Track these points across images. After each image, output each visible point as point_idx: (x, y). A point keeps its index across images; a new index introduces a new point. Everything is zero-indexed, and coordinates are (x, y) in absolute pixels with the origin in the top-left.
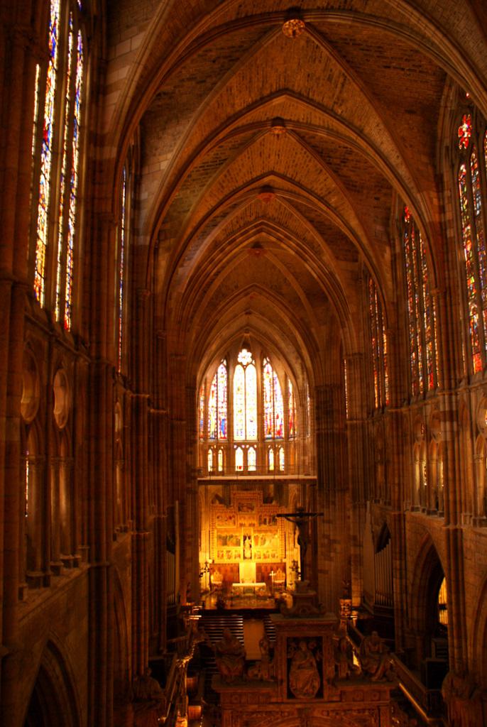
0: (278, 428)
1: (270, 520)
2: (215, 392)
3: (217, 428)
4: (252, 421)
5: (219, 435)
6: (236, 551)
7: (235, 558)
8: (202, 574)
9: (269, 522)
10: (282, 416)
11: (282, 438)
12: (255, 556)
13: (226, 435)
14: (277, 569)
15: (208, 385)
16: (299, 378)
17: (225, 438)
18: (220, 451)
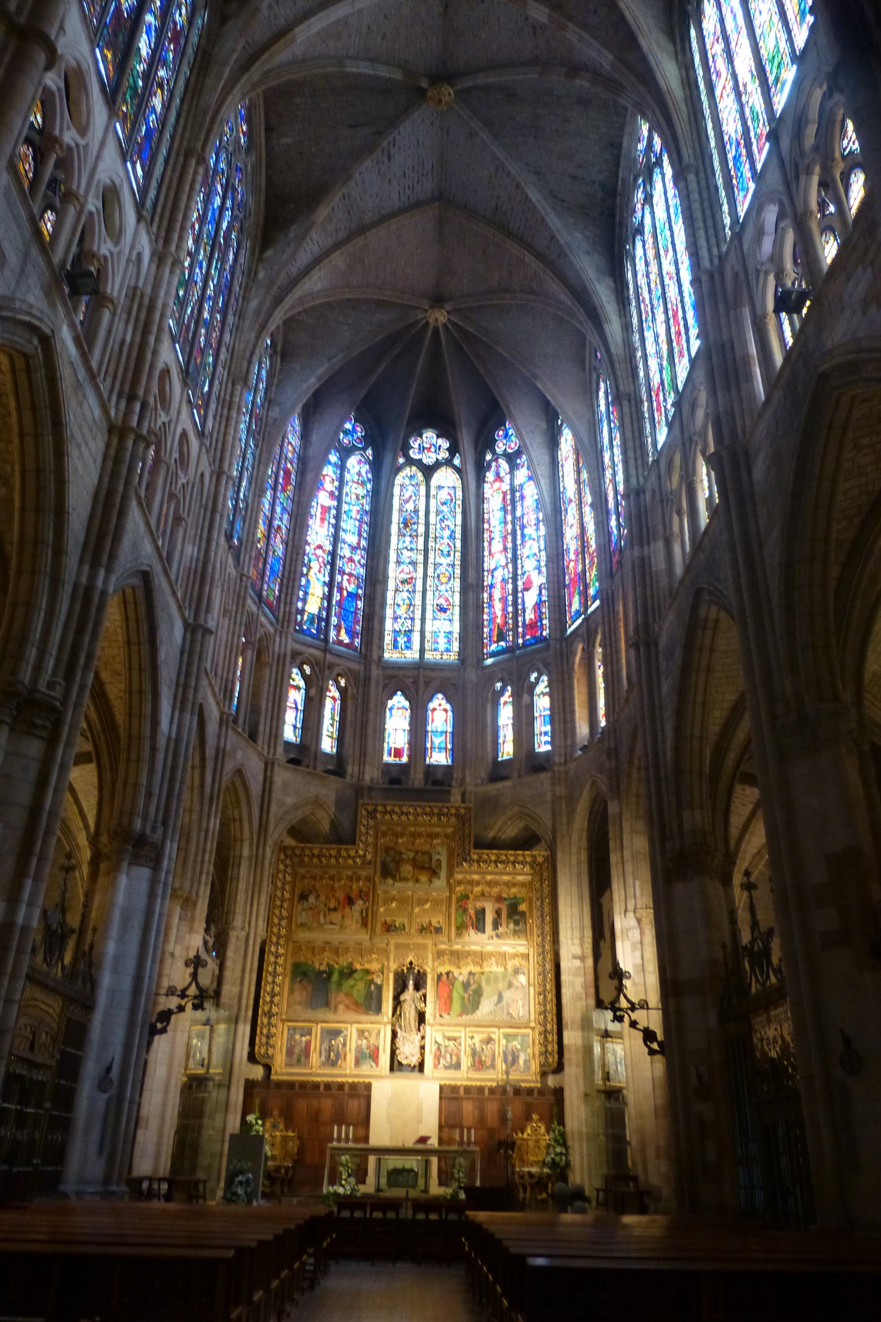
0: (530, 615)
1: (498, 913)
2: (333, 512)
3: (329, 609)
4: (443, 610)
5: (333, 634)
6: (361, 1033)
7: (357, 1063)
8: (166, 1016)
9: (496, 925)
10: (539, 580)
11: (545, 638)
12: (438, 1057)
13: (357, 642)
14: (529, 1118)
15: (310, 476)
16: (608, 321)
17: (349, 646)
18: (334, 692)
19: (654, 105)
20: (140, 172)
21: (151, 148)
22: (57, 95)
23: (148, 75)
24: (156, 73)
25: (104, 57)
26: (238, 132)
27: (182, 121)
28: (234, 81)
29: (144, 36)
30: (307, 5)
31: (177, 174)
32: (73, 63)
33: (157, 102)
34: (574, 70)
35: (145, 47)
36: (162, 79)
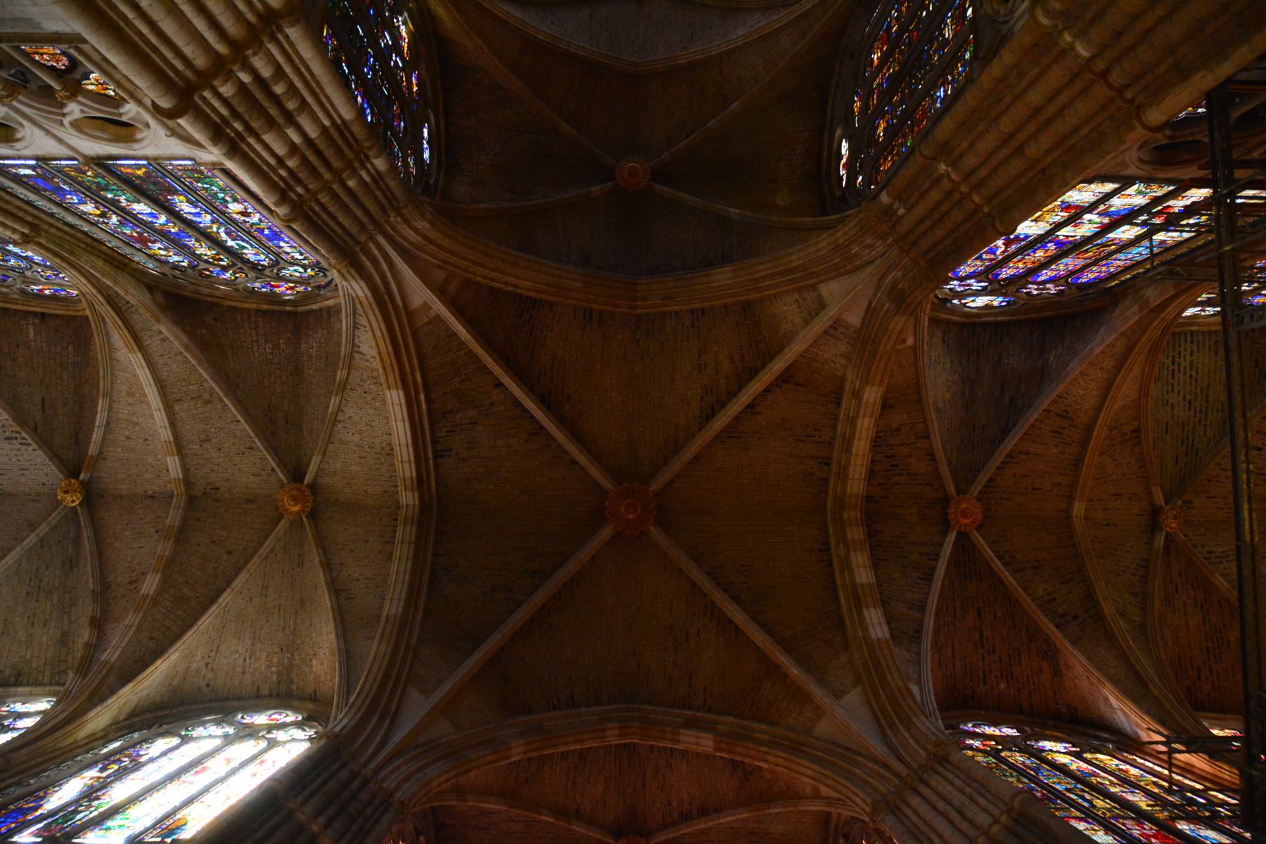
19: (70, 710)
20: (23, 172)
21: (45, 190)
22: (115, 111)
23: (115, 203)
24: (115, 213)
25: (139, 167)
26: (45, 284)
27: (67, 229)
28: (99, 287)
29: (149, 210)
30: (159, 367)
31: (15, 211)
32: (139, 136)
33: (89, 208)
34: (99, 625)
35: (140, 208)
36: (109, 218)
